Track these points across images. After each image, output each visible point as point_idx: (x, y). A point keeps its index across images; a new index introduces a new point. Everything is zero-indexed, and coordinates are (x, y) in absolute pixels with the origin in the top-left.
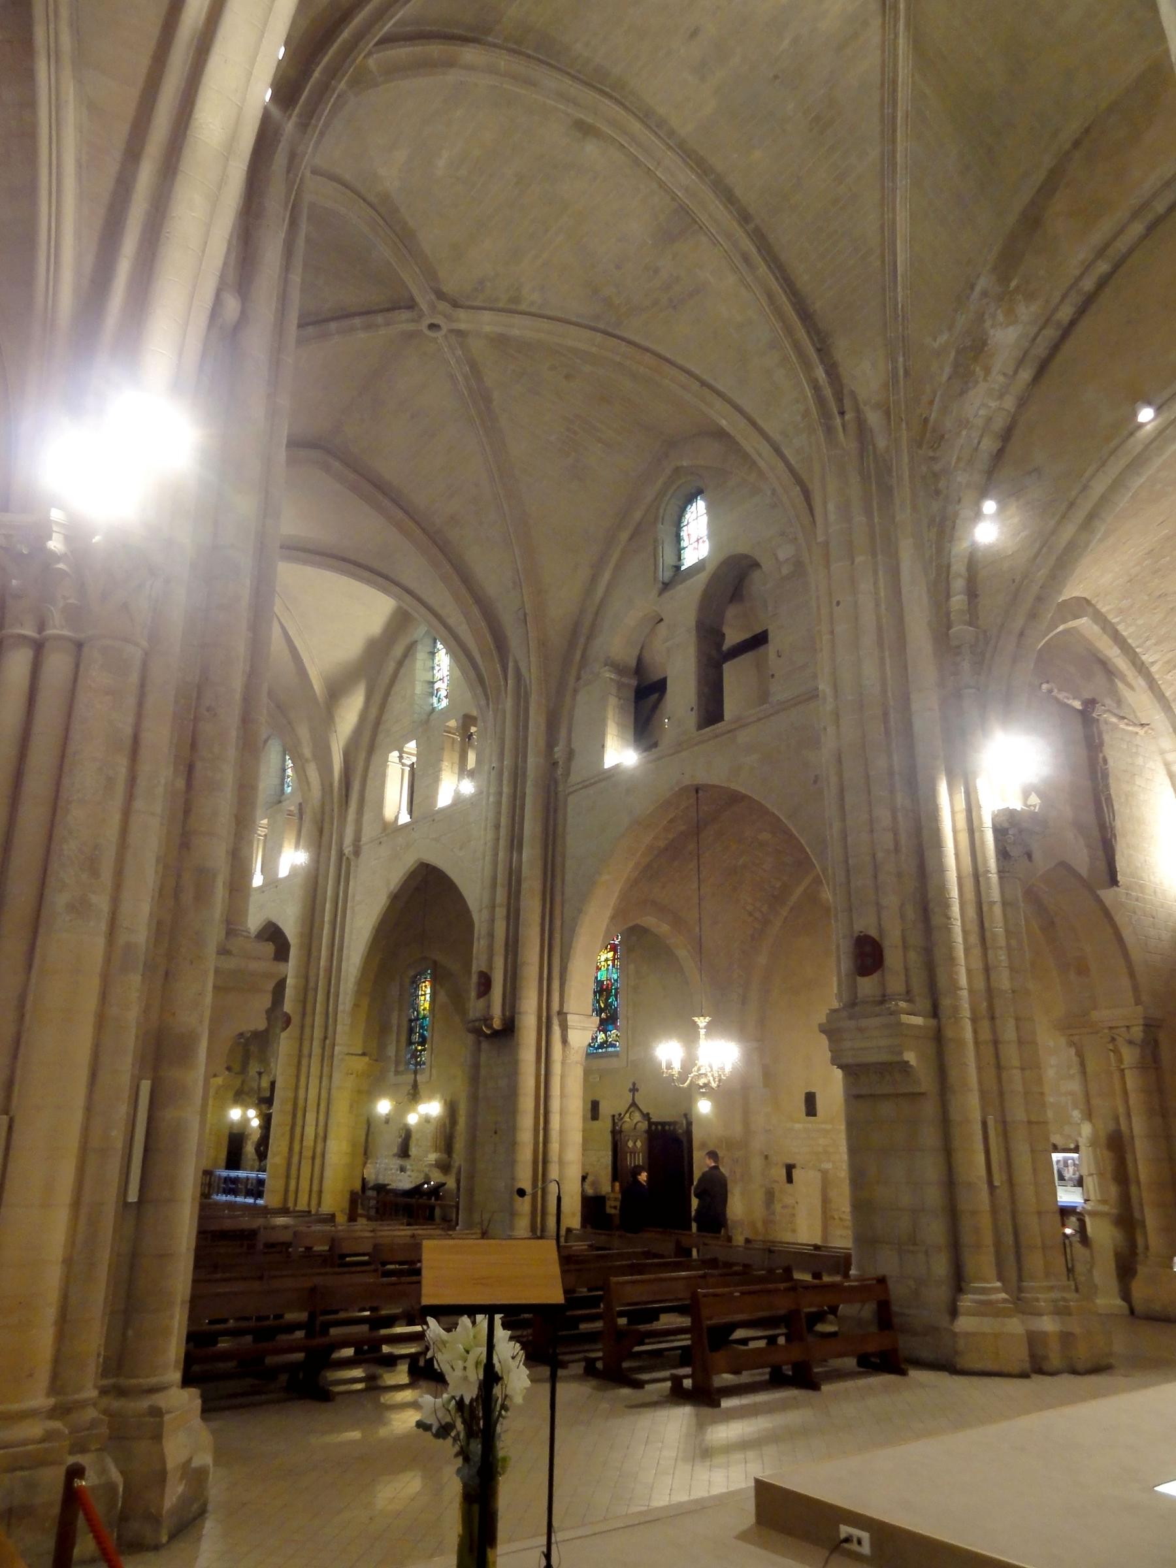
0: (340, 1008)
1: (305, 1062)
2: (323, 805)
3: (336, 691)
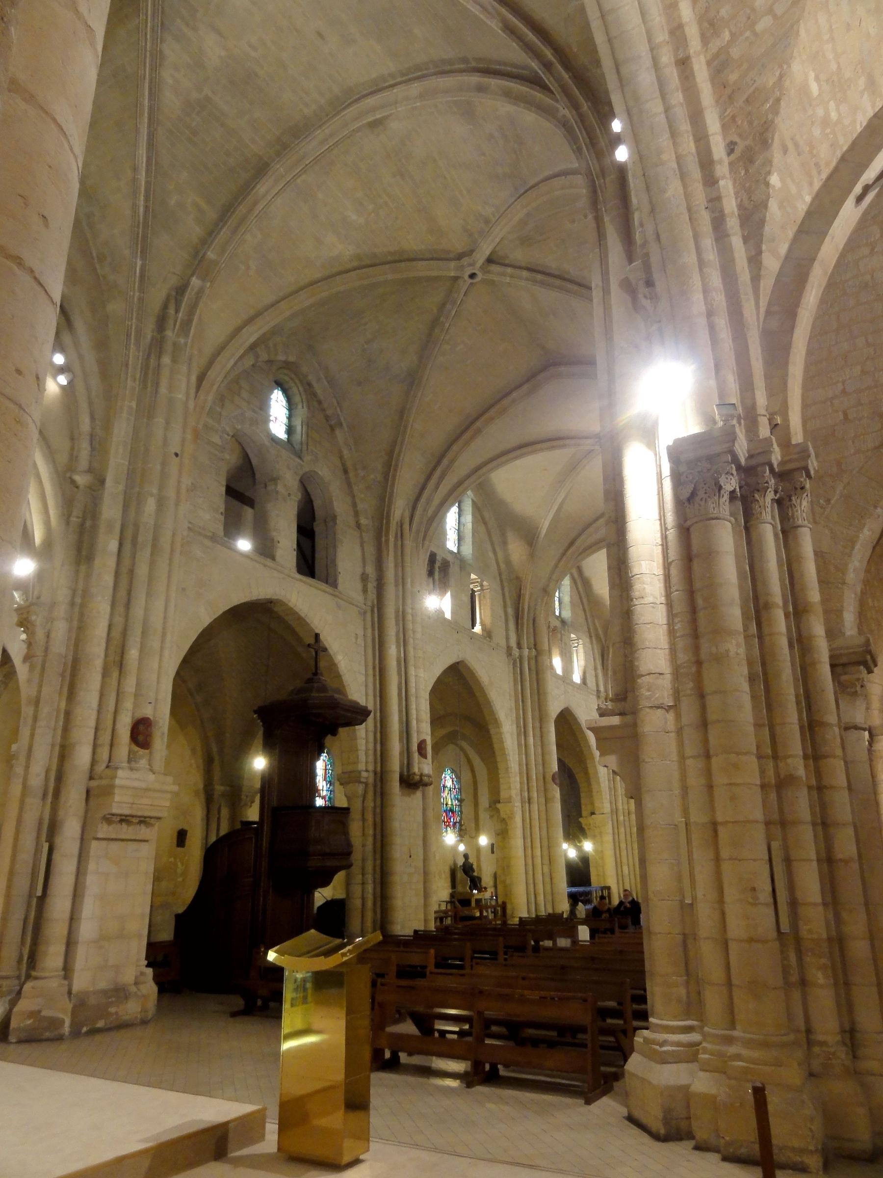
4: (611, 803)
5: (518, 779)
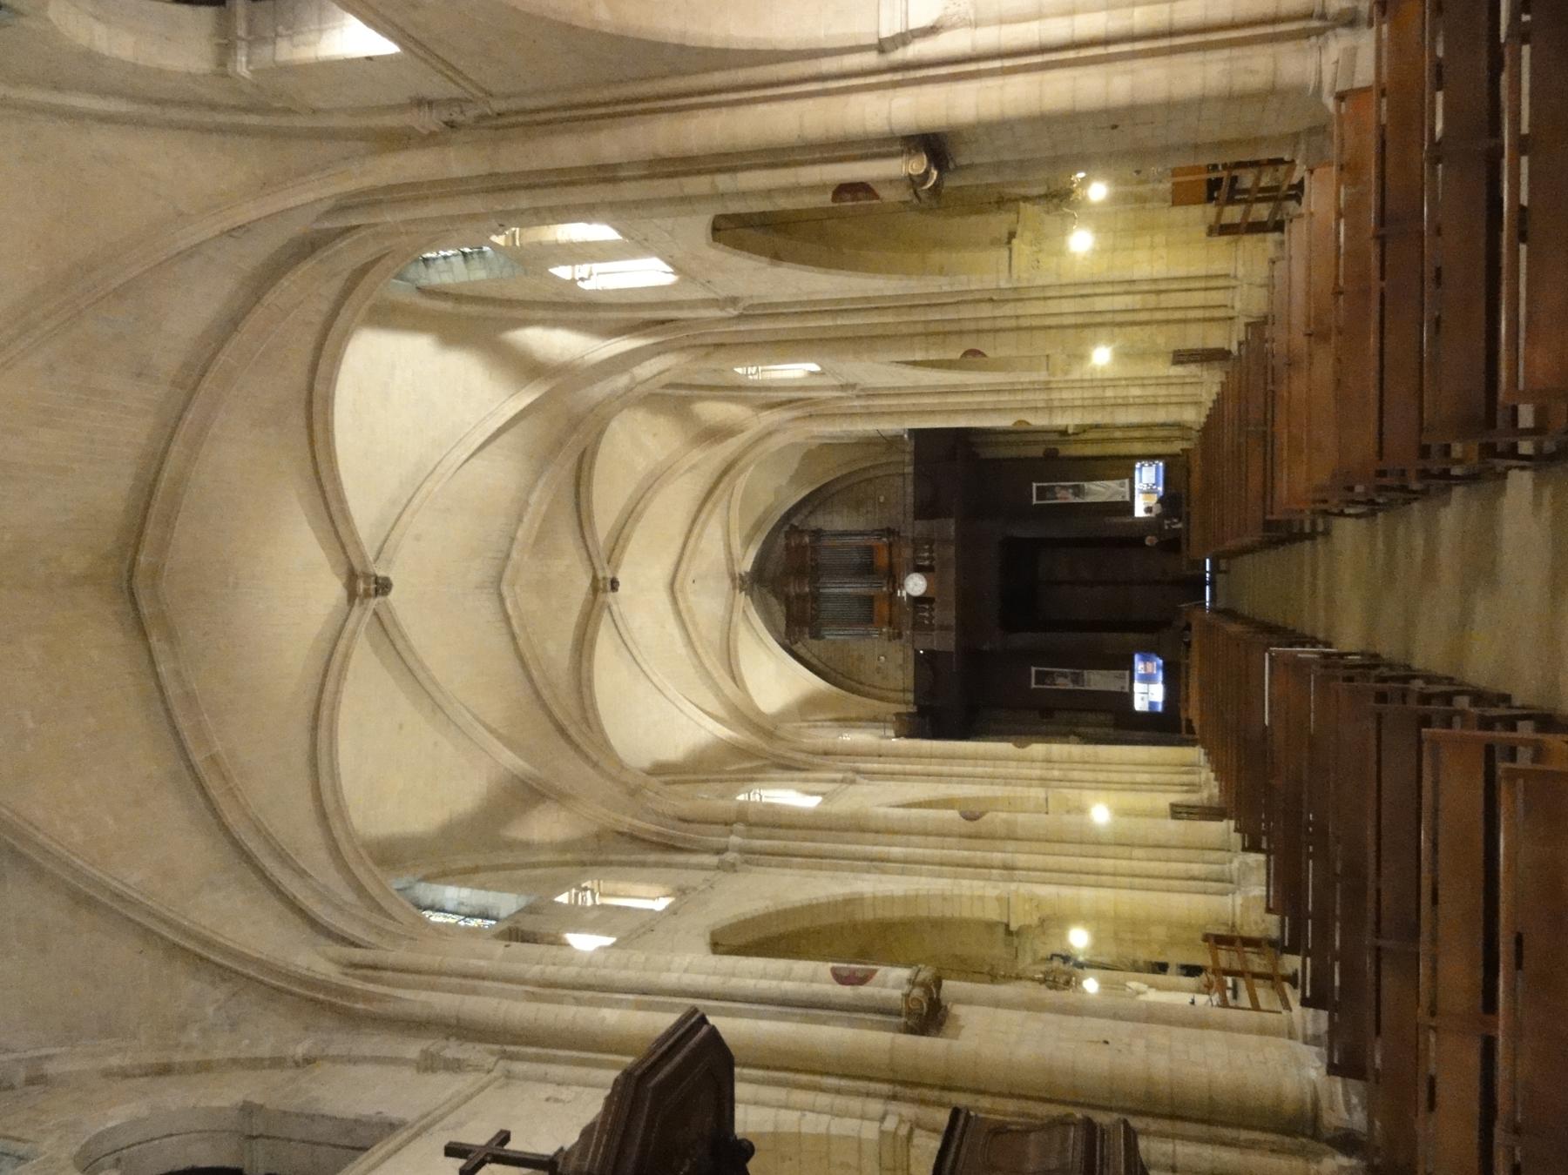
0: (946, 288)
1: (1024, 323)
2: (682, 349)
3: (530, 369)
5: (965, 882)
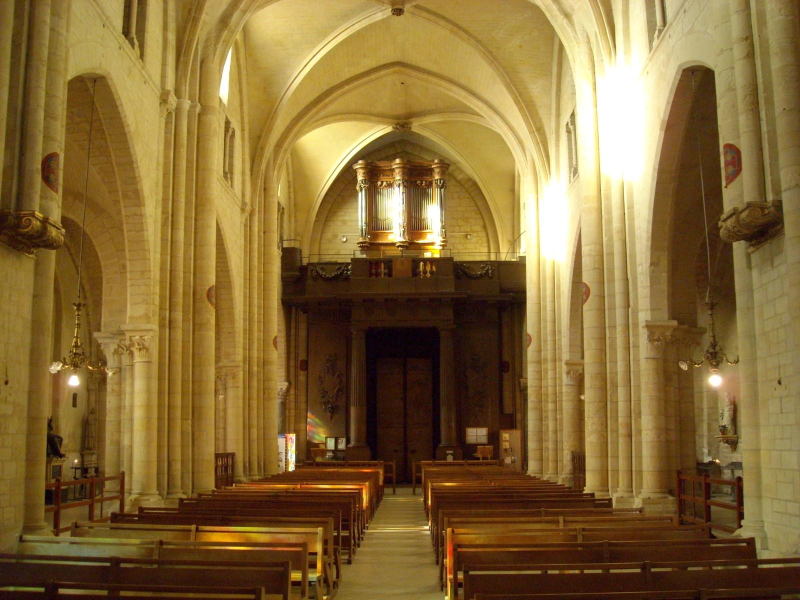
4: (244, 349)
